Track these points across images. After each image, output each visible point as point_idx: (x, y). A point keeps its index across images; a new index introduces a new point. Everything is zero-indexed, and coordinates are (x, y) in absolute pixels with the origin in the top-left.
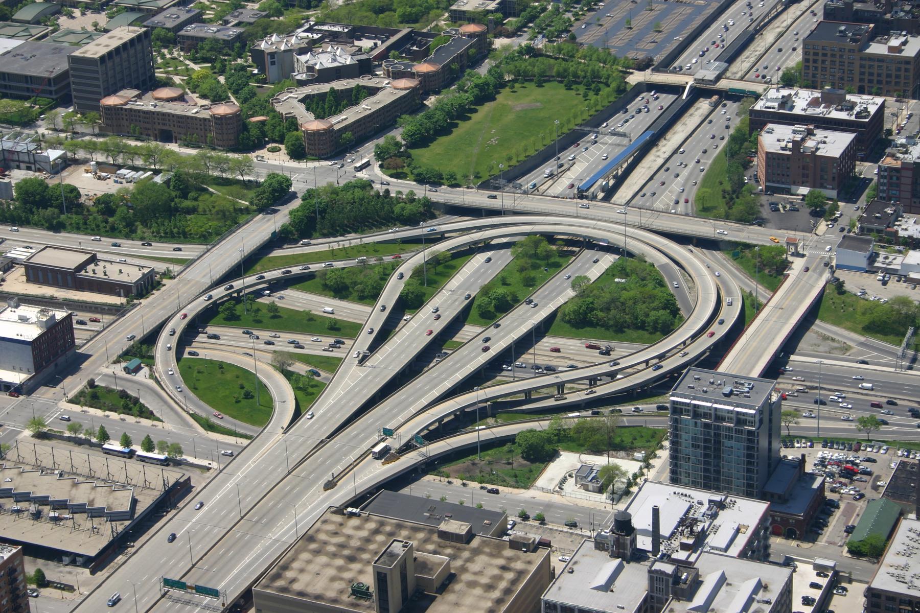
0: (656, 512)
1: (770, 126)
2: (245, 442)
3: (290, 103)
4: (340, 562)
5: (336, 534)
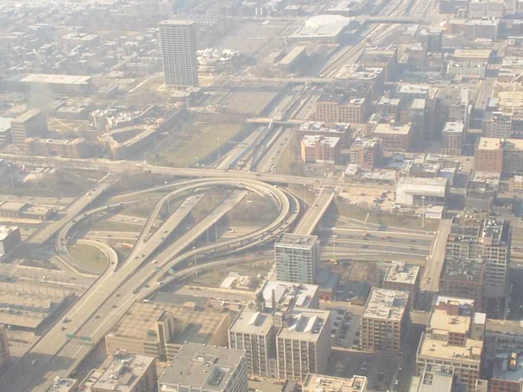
0: (273, 291)
1: (306, 136)
2: (98, 276)
3: (106, 138)
4: (142, 322)
5: (139, 311)
